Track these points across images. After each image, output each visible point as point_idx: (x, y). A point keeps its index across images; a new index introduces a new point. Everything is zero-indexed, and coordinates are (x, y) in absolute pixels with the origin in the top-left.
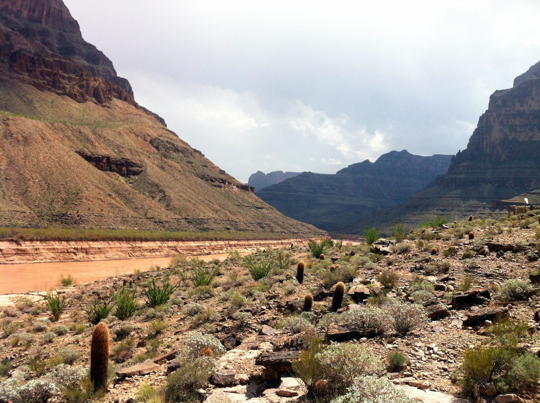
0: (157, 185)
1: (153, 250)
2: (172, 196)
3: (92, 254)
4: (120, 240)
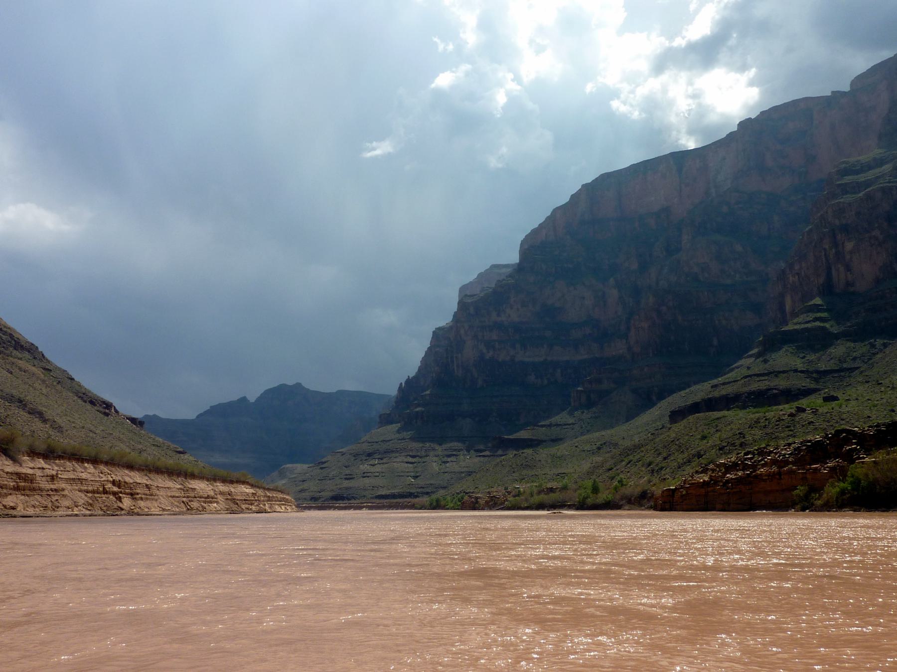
0: (20, 401)
1: (209, 499)
2: (57, 419)
3: (141, 499)
4: (158, 470)
